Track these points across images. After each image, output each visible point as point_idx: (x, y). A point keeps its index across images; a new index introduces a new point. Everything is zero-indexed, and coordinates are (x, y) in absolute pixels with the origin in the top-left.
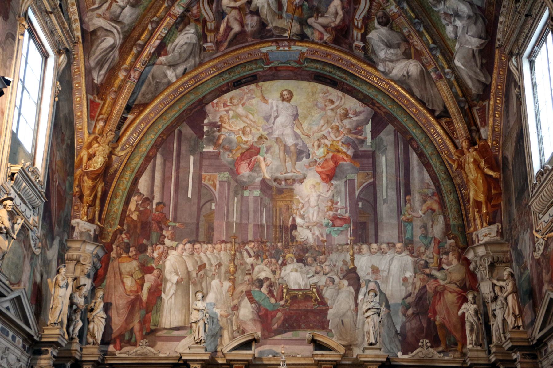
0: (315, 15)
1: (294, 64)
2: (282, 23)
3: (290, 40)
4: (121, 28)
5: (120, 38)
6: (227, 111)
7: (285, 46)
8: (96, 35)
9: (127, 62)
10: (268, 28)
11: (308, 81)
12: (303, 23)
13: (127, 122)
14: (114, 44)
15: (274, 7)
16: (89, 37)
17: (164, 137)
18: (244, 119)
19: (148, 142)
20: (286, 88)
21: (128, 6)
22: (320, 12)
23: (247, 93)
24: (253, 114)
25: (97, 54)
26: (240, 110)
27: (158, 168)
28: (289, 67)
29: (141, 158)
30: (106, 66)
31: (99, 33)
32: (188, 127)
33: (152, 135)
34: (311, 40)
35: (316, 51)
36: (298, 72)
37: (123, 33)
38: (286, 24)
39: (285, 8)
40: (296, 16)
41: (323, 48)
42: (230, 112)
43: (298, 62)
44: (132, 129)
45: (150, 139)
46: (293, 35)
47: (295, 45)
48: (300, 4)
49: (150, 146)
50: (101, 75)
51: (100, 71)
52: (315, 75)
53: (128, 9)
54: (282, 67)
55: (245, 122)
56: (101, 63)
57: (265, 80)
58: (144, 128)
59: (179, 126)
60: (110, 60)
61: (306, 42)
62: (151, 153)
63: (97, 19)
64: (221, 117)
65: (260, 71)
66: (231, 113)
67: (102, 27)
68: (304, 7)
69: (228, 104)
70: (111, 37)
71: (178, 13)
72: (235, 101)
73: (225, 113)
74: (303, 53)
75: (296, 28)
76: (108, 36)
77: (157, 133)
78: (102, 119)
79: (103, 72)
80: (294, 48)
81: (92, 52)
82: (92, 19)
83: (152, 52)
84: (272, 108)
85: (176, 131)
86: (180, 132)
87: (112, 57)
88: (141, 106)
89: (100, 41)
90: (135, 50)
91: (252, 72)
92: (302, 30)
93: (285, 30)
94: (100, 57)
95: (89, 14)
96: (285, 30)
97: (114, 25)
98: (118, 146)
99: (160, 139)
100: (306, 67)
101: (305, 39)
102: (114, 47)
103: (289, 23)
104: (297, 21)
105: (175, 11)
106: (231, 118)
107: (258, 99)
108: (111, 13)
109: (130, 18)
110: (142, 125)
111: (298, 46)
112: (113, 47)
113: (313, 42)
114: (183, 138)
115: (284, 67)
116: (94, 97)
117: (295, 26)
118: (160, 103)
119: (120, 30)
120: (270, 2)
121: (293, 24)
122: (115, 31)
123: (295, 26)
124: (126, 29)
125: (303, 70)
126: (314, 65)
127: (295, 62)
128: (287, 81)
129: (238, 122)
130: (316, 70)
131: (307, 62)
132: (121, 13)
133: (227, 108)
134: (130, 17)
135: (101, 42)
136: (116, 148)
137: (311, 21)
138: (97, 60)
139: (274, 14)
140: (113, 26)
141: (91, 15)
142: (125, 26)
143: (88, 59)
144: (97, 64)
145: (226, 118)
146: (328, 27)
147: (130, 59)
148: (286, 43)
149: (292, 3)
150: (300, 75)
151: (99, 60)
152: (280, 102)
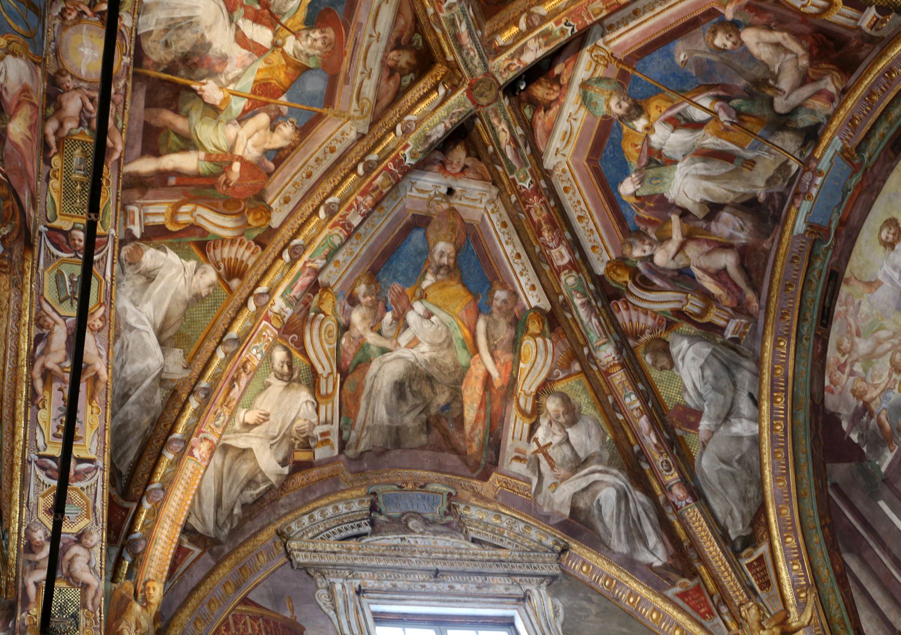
0: (769, 92)
1: (854, 181)
2: (767, 165)
3: (805, 165)
4: (600, 462)
5: (616, 476)
6: (852, 373)
7: (811, 182)
8: (580, 511)
9: (659, 492)
10: (762, 197)
11: (891, 169)
12: (782, 122)
13: (768, 560)
14: (618, 491)
15: (718, 168)
16: (579, 525)
17: (828, 521)
18: (880, 350)
19: (820, 554)
20: (878, 227)
21: (568, 430)
22: (765, 81)
23: (847, 311)
24: (881, 328)
25: (614, 531)
26: (863, 346)
27: (864, 577)
28: (853, 194)
29: (834, 591)
30: (648, 529)
31: (581, 505)
32: (835, 465)
33: (815, 539)
34: (825, 121)
35: (851, 121)
36: (870, 181)
37: (610, 464)
38: (772, 158)
39: (732, 147)
40: (760, 131)
41: (849, 104)
42: (855, 369)
43: (856, 169)
44: (781, 564)
45: (818, 548)
46: (801, 154)
47: (818, 161)
48: (734, 115)
49: (827, 558)
50: (655, 548)
51: (646, 544)
52: (892, 149)
53: (572, 433)
54: (845, 210)
55: (885, 353)
56: (635, 534)
57: (847, 260)
58: (797, 541)
59: (826, 479)
60: (643, 515)
61: (823, 133)
62: (837, 567)
63: (556, 493)
64: (853, 392)
65: (831, 258)
66: (858, 368)
67: (575, 493)
68: (743, 109)
69: (843, 360)
70: (602, 489)
71: (610, 359)
72: (846, 344)
73: (852, 378)
74: (844, 150)
75: (788, 142)
76: (597, 492)
77: (815, 527)
78: (719, 601)
79: (652, 540)
80: (824, 165)
81: (603, 537)
82: (551, 500)
83: (655, 441)
84: (892, 280)
85: (831, 493)
86: (835, 486)
87: (640, 509)
88: (759, 519)
89: (596, 512)
90: (646, 467)
91: (824, 274)
92: (796, 130)
93: (785, 166)
94: (622, 529)
95: (540, 499)
96: (785, 166)
97: (586, 471)
98: (788, 612)
99: (826, 529)
100: (870, 158)
101: (819, 132)
102: (626, 494)
103: (773, 151)
104: (772, 134)
105: (605, 361)
106: (864, 375)
107: (865, 296)
108: (562, 465)
109: (593, 439)
110: (789, 540)
111: (822, 155)
112: (623, 497)
113: (830, 118)
114: (846, 491)
115: (847, 205)
116: (681, 585)
117: (783, 141)
118: (775, 481)
119: (600, 468)
120: (704, 172)
121: (779, 144)
122: (597, 476)
123: (783, 141)
124: (606, 455)
125: (872, 168)
126: (875, 140)
127: (851, 177)
128: (871, 216)
129: (877, 366)
130: (886, 140)
131: (864, 151)
132: (572, 448)
133: (847, 370)
134: (590, 437)
135: (600, 510)
136: (787, 618)
137: (781, 105)
138: (623, 537)
139: (735, 174)
140: (585, 475)
141: (544, 499)
142: (600, 455)
143: (610, 549)
144: (630, 540)
145: (861, 385)
146: (807, 75)
147: (655, 485)
148: (808, 176)
149: (727, 129)
150: (875, 180)
151: (626, 533)
152: (892, 254)
